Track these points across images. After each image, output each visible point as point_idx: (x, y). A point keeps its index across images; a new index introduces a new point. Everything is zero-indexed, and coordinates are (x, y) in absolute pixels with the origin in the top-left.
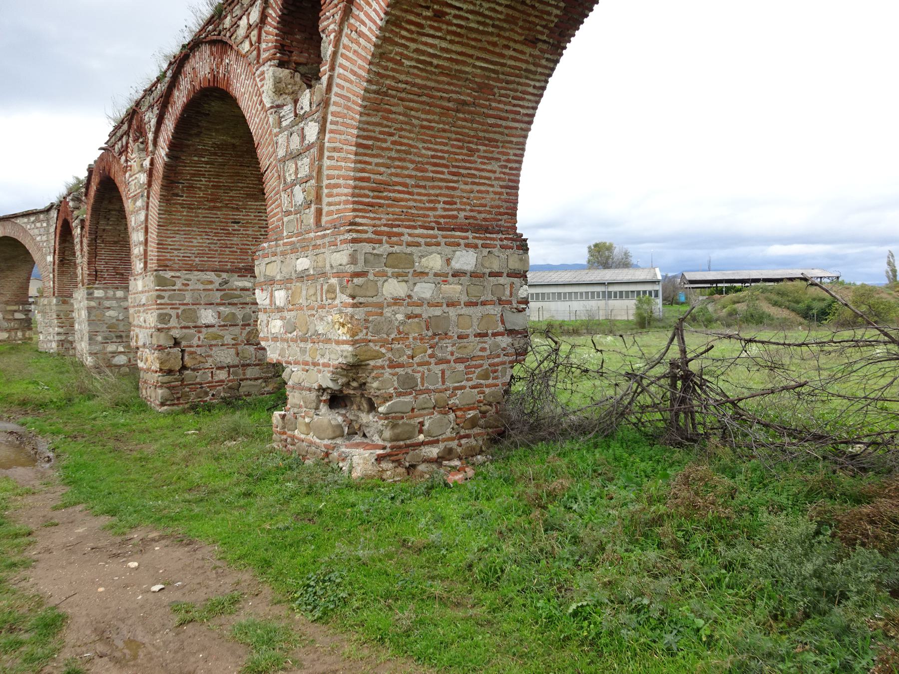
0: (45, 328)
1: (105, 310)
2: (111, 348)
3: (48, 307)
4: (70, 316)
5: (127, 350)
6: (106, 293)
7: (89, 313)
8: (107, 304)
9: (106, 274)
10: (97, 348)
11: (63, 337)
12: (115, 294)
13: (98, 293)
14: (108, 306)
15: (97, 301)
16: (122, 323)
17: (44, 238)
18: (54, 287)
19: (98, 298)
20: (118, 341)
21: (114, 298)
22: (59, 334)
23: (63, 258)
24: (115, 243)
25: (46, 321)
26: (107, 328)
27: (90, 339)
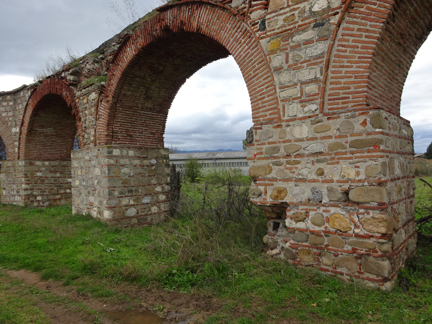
0: (9, 185)
1: (121, 167)
2: (125, 201)
3: (12, 169)
4: (35, 175)
5: (136, 203)
6: (122, 152)
7: (109, 170)
8: (122, 161)
9: (120, 135)
10: (114, 202)
11: (29, 192)
12: (128, 153)
13: (116, 152)
14: (123, 163)
15: (115, 159)
16: (133, 179)
17: (11, 114)
18: (19, 152)
19: (116, 156)
20: (130, 195)
21: (128, 157)
22: (26, 189)
23: (32, 129)
24: (131, 107)
25: (10, 179)
26: (122, 183)
27: (110, 194)
